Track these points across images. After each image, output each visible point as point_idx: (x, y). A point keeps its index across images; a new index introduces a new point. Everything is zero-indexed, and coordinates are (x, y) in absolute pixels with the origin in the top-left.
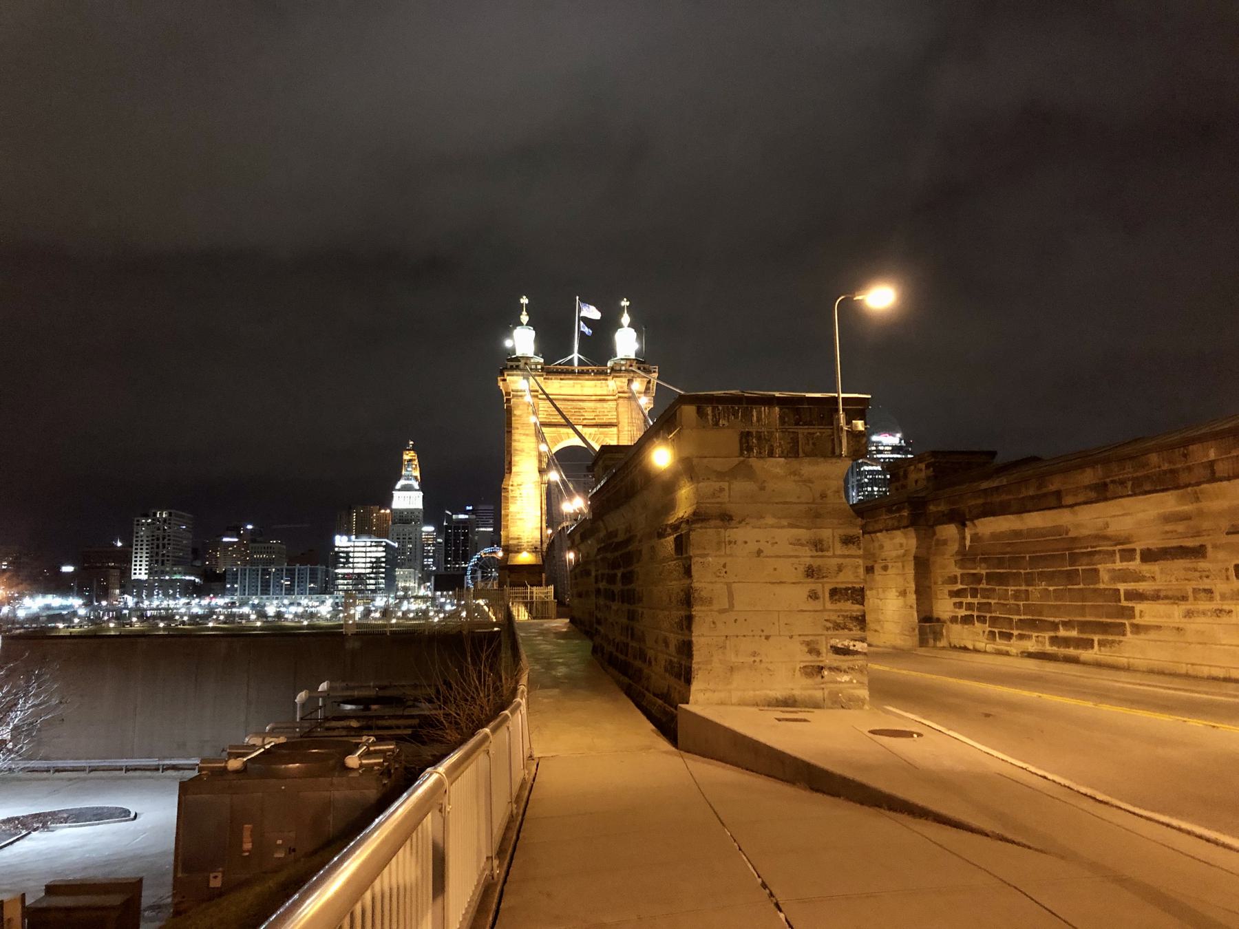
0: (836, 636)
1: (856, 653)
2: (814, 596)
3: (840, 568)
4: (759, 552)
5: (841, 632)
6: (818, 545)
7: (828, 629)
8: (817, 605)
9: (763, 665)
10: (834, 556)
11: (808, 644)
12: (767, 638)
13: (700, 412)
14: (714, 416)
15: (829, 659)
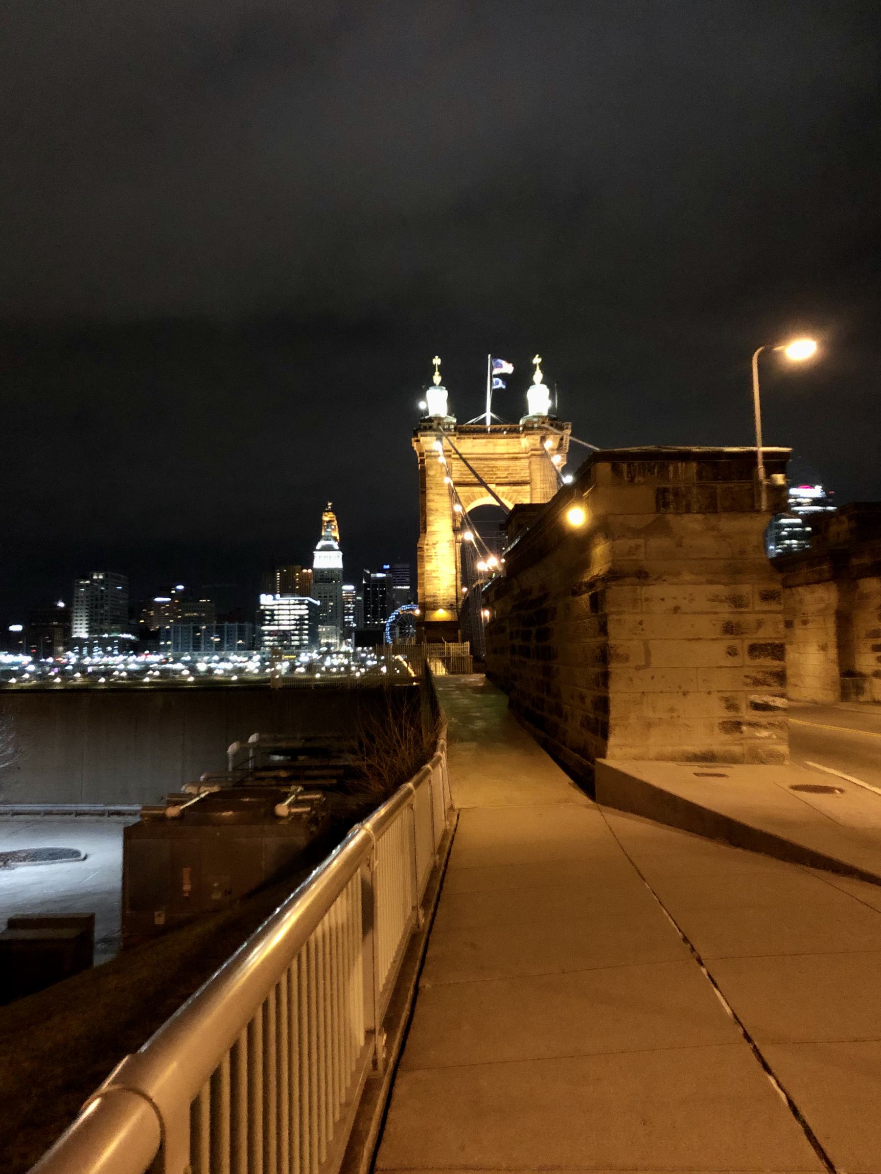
0: (756, 692)
3: (759, 624)
4: (676, 609)
5: (759, 688)
6: (737, 602)
7: (747, 685)
11: (727, 700)
12: (685, 694)
13: (615, 469)
14: (629, 472)
15: (748, 715)
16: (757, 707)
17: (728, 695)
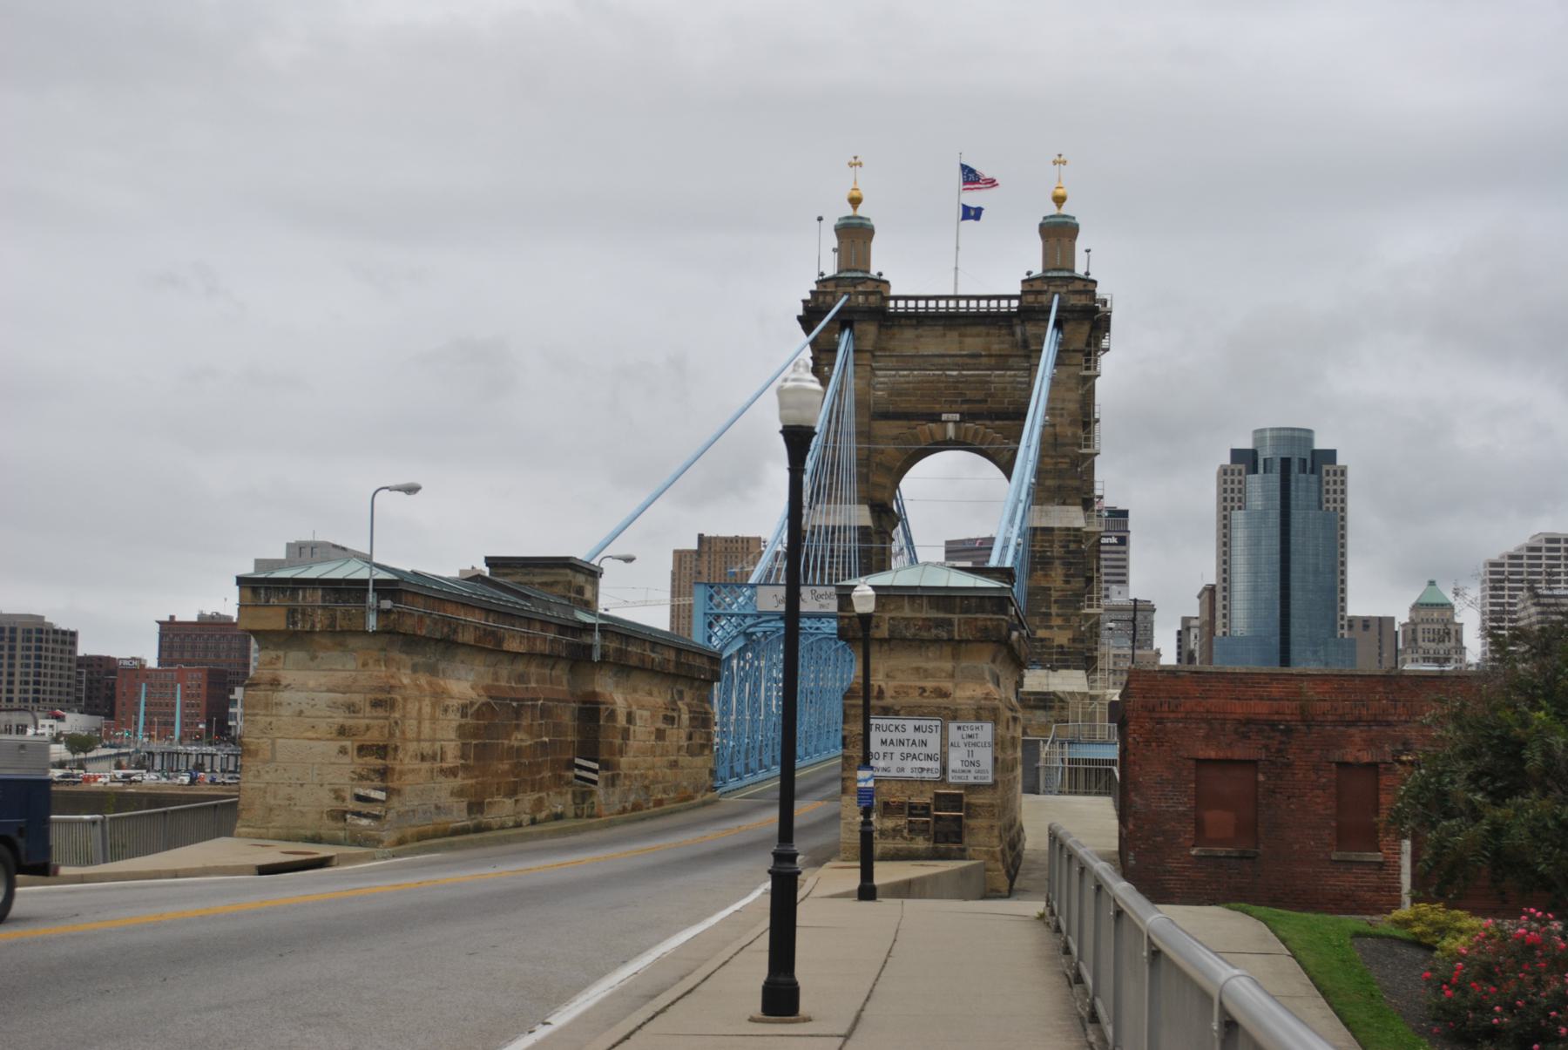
2: (343, 751)
4: (301, 712)
6: (351, 708)
8: (347, 760)
15: (352, 805)
16: (359, 798)
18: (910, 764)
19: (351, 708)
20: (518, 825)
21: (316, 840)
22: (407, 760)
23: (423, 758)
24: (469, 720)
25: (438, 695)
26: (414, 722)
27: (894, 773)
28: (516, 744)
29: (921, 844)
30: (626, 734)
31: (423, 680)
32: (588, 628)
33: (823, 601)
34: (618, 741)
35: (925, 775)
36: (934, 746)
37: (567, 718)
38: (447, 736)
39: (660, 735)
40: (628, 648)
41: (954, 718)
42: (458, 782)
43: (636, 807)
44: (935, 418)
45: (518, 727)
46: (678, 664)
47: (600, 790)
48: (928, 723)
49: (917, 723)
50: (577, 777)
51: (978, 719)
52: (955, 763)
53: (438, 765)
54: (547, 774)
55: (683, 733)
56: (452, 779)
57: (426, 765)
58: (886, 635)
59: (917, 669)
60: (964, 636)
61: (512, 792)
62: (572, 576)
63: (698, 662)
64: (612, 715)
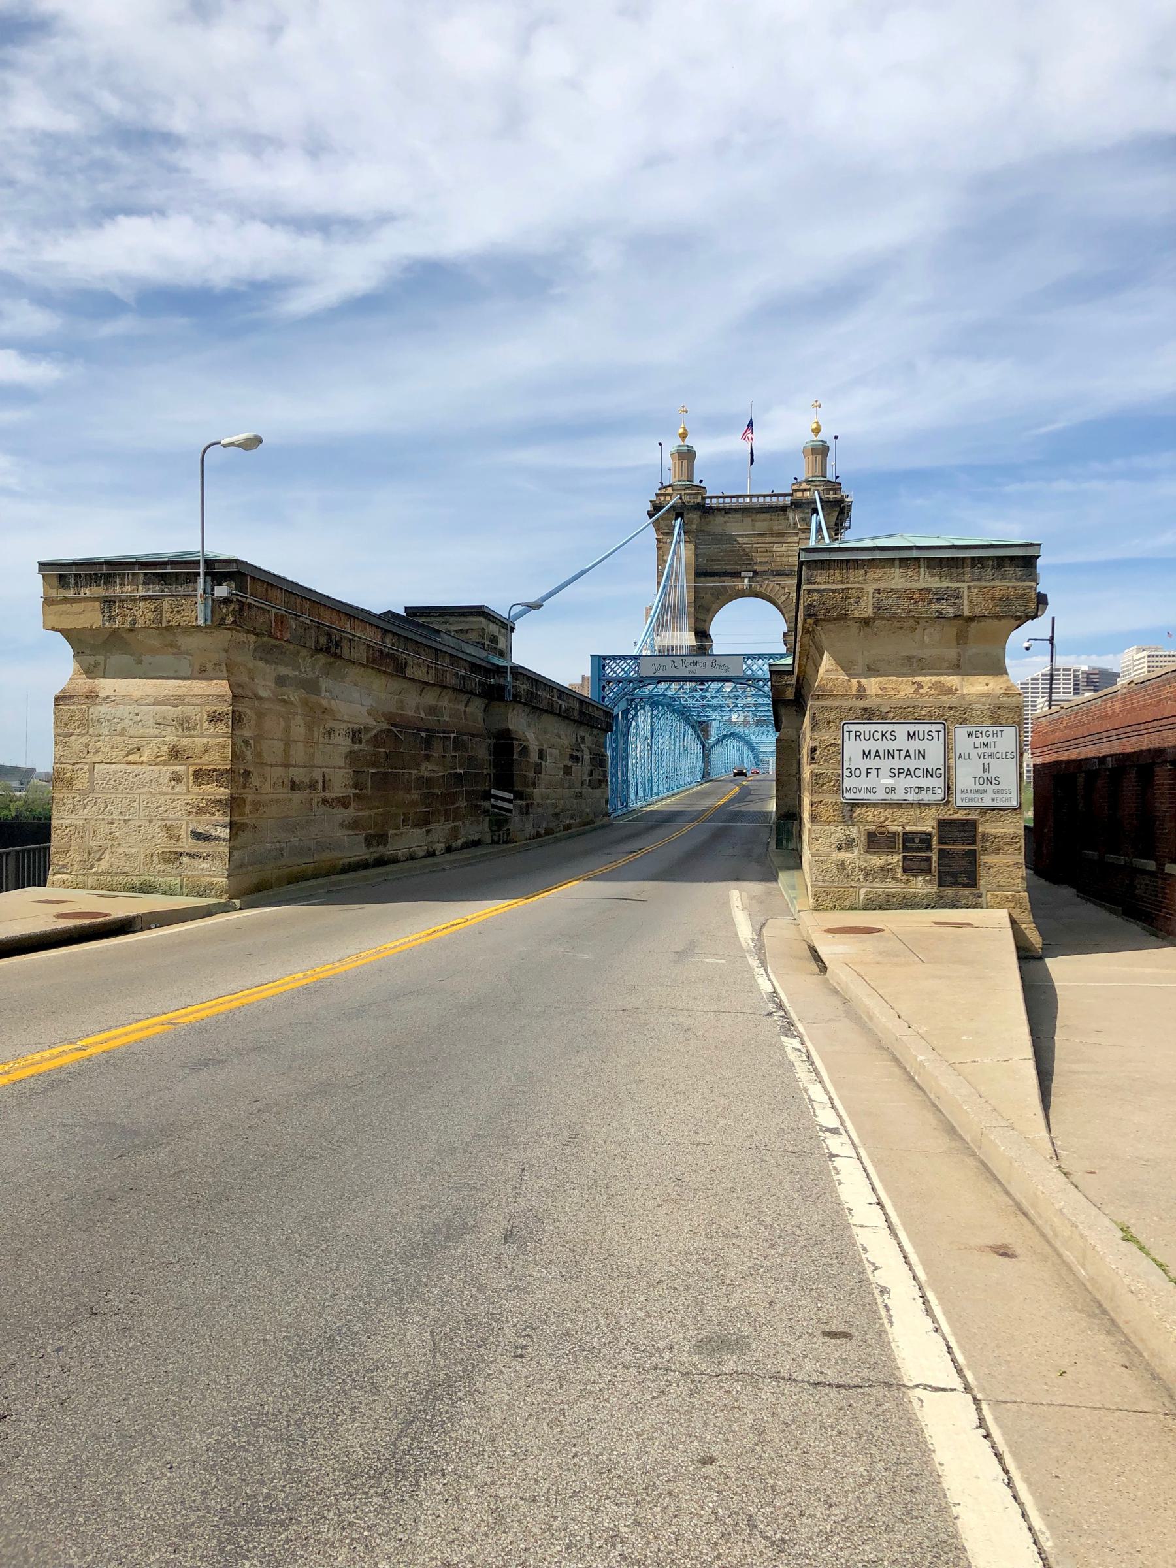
1: (219, 839)
2: (176, 778)
6: (185, 724)
8: (181, 788)
9: (120, 850)
10: (202, 735)
15: (188, 844)
16: (197, 836)
17: (169, 823)
18: (904, 782)
19: (185, 724)
20: (431, 854)
21: (147, 889)
22: (267, 788)
23: (294, 786)
24: (364, 746)
25: (317, 715)
26: (280, 745)
27: (880, 795)
28: (426, 774)
29: (920, 886)
30: (538, 769)
31: (294, 695)
32: (499, 671)
33: (691, 668)
34: (531, 774)
35: (925, 797)
36: (935, 759)
37: (482, 751)
38: (334, 761)
39: (567, 771)
40: (537, 692)
41: (963, 722)
42: (352, 812)
43: (549, 832)
44: (737, 574)
45: (427, 757)
46: (581, 713)
47: (515, 818)
48: (927, 728)
49: (912, 728)
50: (494, 806)
51: (997, 722)
52: (964, 778)
53: (319, 794)
54: (462, 804)
55: (587, 768)
56: (342, 810)
57: (298, 796)
58: (869, 612)
59: (910, 659)
60: (977, 612)
61: (424, 822)
62: (483, 627)
63: (596, 714)
64: (525, 751)
